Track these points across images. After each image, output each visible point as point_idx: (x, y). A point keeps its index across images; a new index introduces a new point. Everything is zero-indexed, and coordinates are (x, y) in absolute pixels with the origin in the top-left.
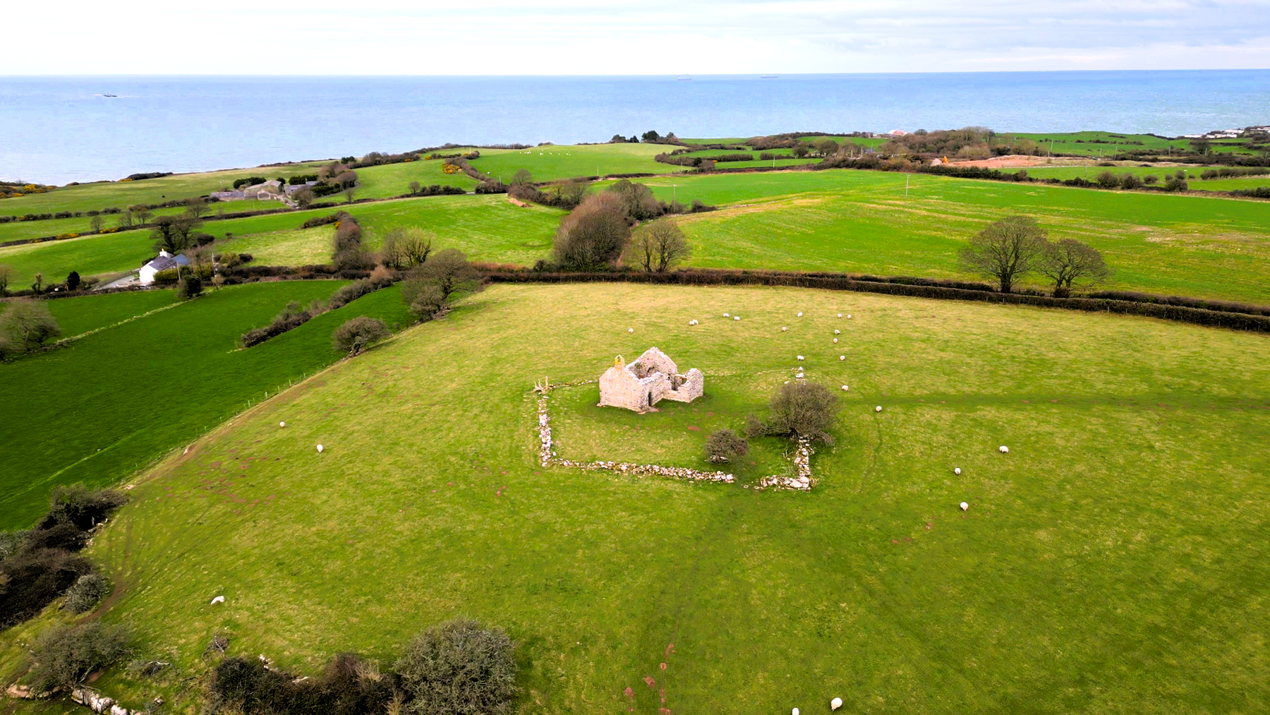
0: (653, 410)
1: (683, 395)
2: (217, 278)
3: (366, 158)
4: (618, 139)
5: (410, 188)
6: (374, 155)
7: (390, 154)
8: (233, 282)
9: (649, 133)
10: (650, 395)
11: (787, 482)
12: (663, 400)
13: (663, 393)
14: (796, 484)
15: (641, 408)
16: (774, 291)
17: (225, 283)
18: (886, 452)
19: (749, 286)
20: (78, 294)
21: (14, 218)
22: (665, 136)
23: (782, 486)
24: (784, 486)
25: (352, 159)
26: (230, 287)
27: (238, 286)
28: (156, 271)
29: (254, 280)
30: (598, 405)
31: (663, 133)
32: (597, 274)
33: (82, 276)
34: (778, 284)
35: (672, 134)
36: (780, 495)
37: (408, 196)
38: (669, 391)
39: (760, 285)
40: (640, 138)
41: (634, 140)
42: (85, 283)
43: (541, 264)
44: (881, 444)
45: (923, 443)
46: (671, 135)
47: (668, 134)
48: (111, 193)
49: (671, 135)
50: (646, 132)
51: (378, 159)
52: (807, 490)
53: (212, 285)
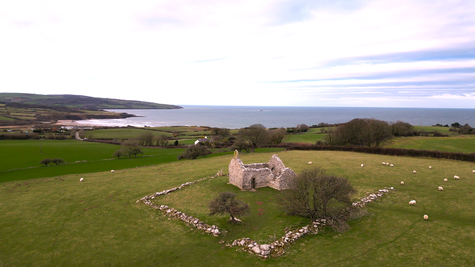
0: (253, 190)
1: (276, 185)
2: (213, 145)
3: (319, 124)
4: (438, 125)
5: (320, 131)
6: (322, 124)
7: (329, 124)
8: (219, 148)
9: (455, 123)
10: (254, 179)
11: (250, 246)
12: (268, 187)
13: (268, 182)
14: (257, 250)
15: (243, 187)
16: (437, 160)
17: (217, 148)
18: (389, 249)
19: (423, 157)
20: (175, 148)
21: (201, 135)
22: (464, 125)
23: (245, 249)
24: (248, 248)
25: (316, 125)
26: (216, 149)
27: (219, 149)
28: (199, 142)
29: (225, 148)
30: (228, 183)
31: (462, 123)
32: (338, 146)
33: (179, 143)
34: (442, 157)
35: (468, 125)
36: (235, 255)
37: (320, 133)
38: (271, 182)
39: (429, 157)
40: (450, 125)
41: (447, 126)
42: (179, 145)
43: (319, 143)
44: (391, 242)
45: (441, 251)
46: (467, 125)
47: (465, 124)
48: (235, 131)
49: (467, 125)
50: (454, 123)
51: (323, 125)
52: (263, 258)
53: (211, 148)
